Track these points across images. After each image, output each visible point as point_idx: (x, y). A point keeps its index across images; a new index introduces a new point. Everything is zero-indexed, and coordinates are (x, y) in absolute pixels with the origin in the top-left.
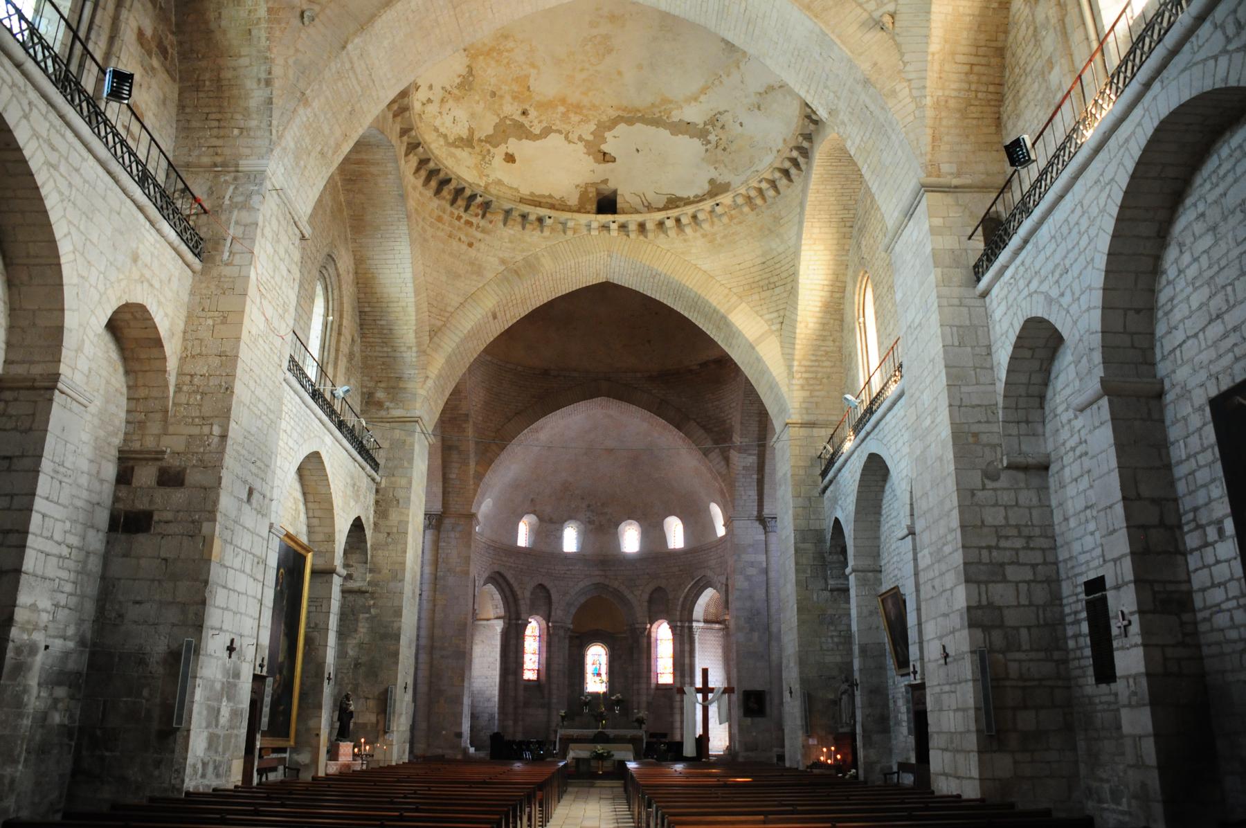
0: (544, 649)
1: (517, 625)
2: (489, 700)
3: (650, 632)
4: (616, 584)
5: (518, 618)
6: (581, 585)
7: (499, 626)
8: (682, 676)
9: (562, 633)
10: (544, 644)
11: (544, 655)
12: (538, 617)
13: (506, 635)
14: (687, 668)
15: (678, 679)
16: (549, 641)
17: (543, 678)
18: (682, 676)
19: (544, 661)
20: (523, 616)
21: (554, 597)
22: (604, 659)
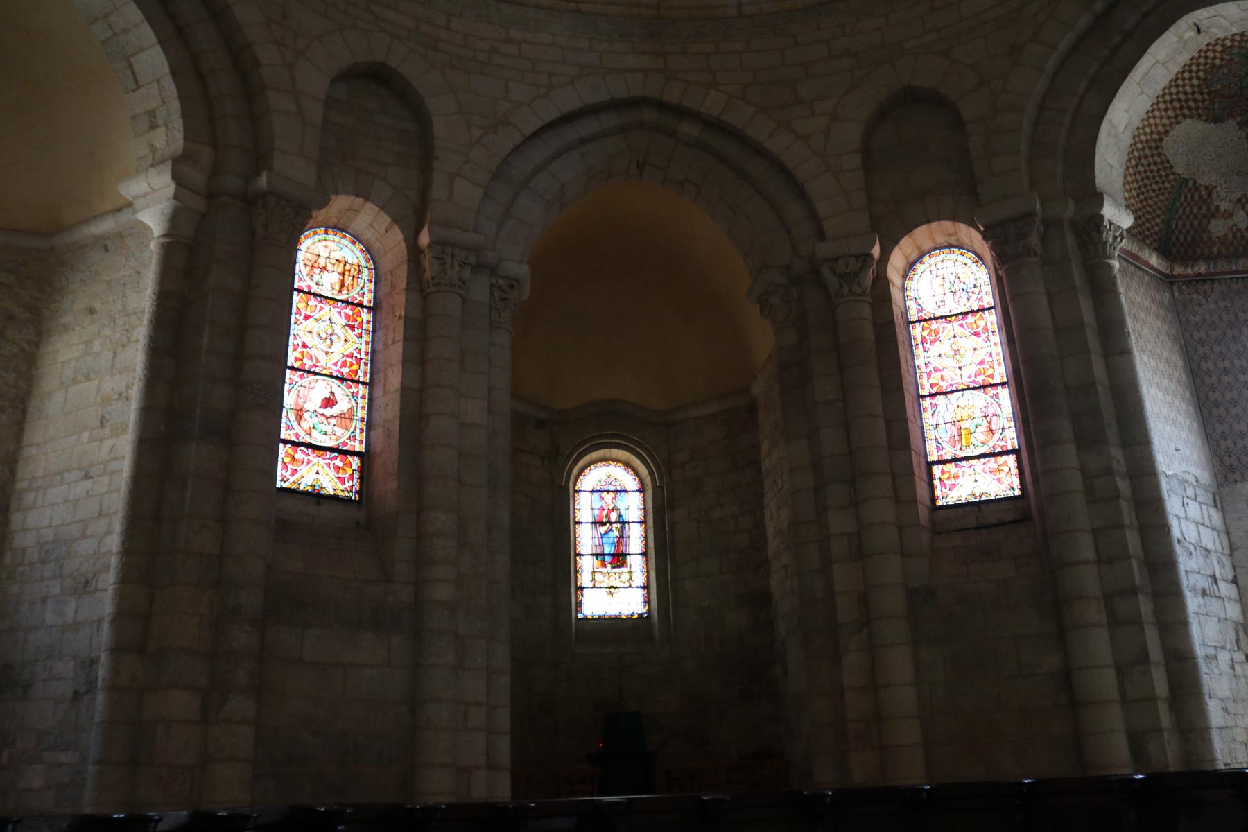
0: (397, 352)
1: (250, 200)
2: (85, 586)
3: (882, 282)
4: (713, 104)
5: (259, 158)
6: (568, 100)
7: (149, 203)
8: (1089, 440)
9: (480, 290)
10: (396, 331)
11: (394, 379)
12: (369, 216)
13: (185, 257)
14: (1104, 398)
15: (1069, 454)
16: (418, 323)
17: (388, 486)
18: (1089, 440)
19: (391, 409)
20: (292, 167)
21: (439, 127)
22: (633, 506)
